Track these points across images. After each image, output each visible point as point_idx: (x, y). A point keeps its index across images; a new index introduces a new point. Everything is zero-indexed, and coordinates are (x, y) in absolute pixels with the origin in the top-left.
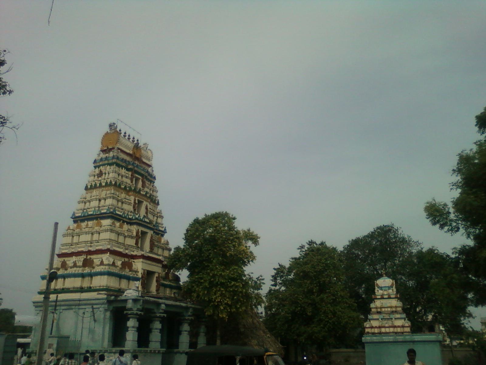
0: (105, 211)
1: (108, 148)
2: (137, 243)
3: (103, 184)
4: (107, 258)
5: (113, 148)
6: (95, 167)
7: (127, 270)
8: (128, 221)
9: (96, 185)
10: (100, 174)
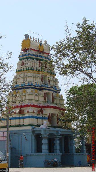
0: (27, 84)
1: (25, 49)
2: (45, 99)
3: (25, 70)
4: (31, 109)
5: (28, 49)
6: (20, 60)
7: (41, 115)
8: (39, 88)
9: (21, 70)
10: (23, 64)
